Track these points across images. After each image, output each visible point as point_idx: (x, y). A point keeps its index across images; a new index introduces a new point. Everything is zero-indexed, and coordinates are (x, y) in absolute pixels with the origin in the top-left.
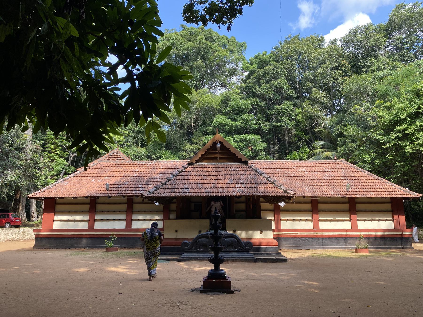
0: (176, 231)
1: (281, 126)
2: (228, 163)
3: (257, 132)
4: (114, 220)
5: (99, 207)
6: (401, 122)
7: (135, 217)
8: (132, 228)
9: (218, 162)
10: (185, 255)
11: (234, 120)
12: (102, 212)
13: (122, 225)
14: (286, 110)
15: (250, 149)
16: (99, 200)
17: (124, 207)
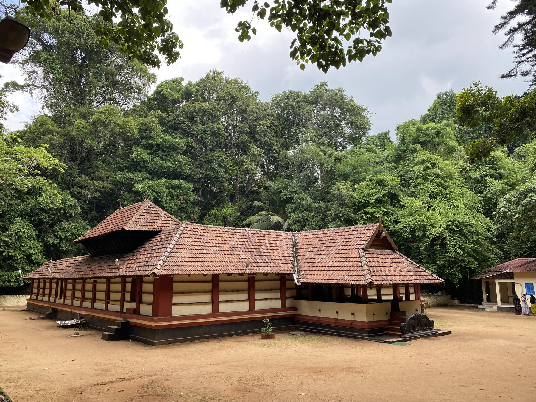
0: (374, 314)
1: (217, 177)
2: (386, 250)
3: (186, 178)
4: (238, 301)
5: (222, 285)
6: (369, 204)
7: (257, 296)
8: (255, 309)
9: (378, 249)
10: (406, 335)
11: (163, 160)
12: (226, 291)
13: (244, 306)
14: (223, 160)
15: (181, 198)
16: (221, 278)
17: (245, 285)
